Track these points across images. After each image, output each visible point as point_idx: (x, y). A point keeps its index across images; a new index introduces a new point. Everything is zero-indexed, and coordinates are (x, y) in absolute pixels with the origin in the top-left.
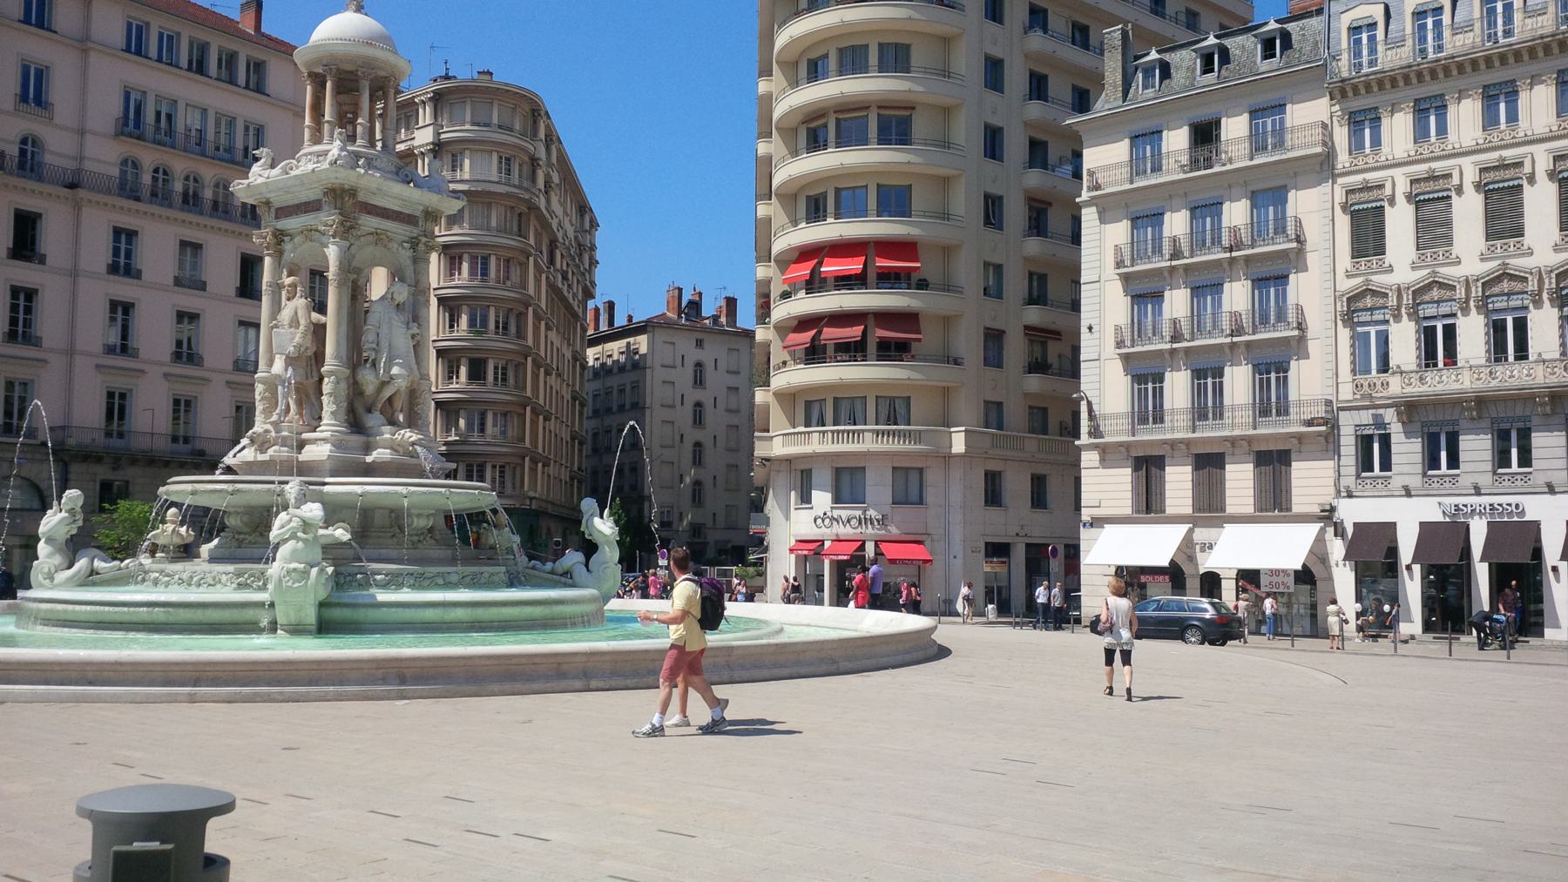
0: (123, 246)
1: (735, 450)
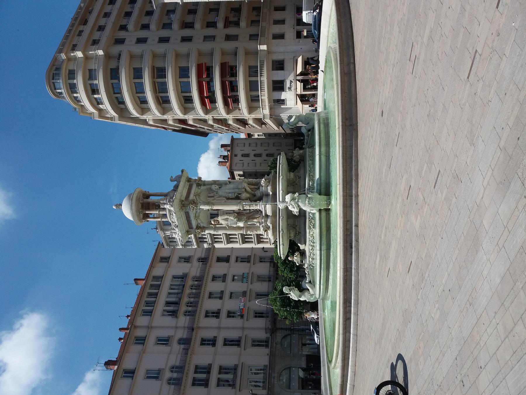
1: (269, 144)
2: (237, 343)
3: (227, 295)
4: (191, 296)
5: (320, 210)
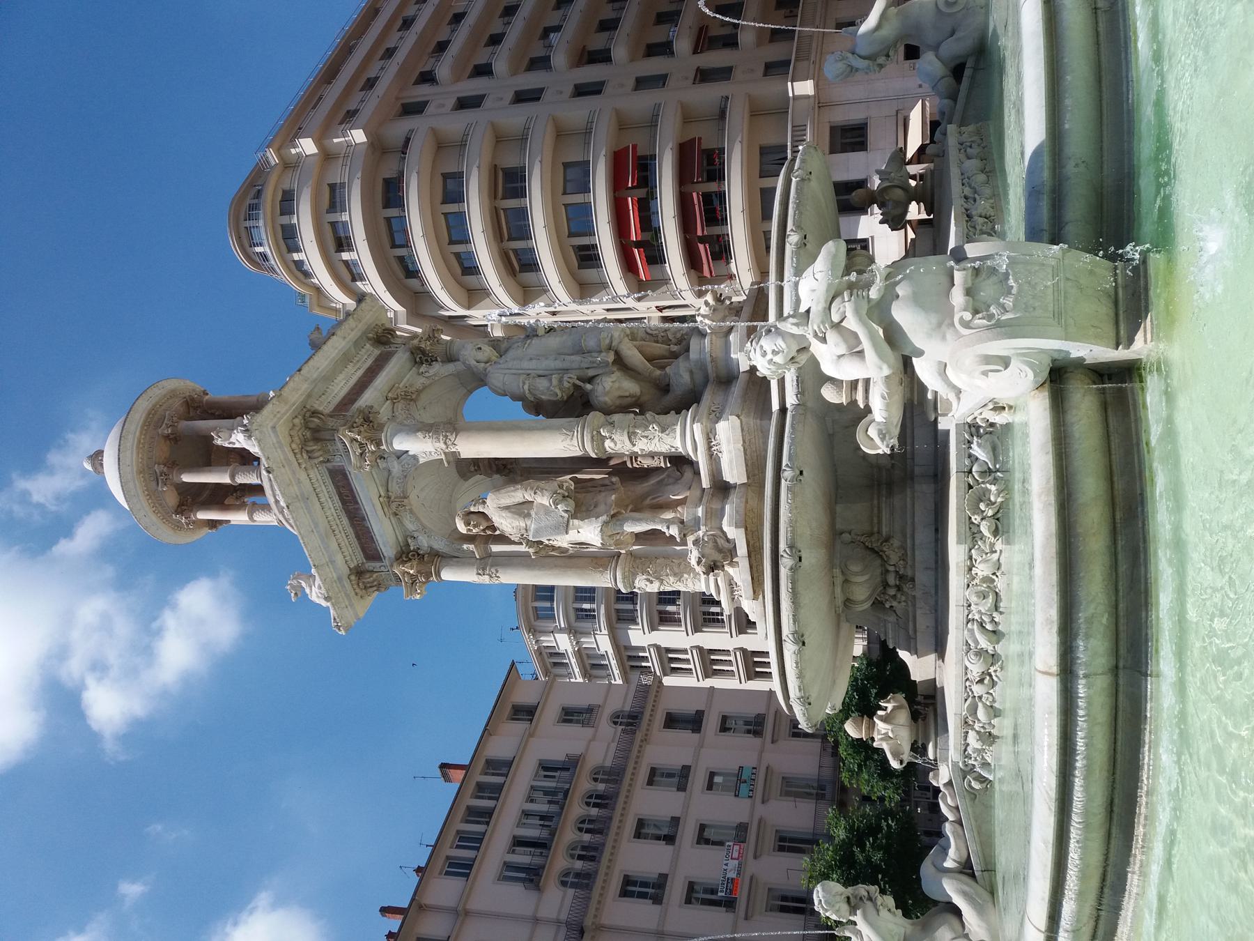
0: (637, 889)
3: (688, 833)
4: (585, 826)
5: (1058, 376)
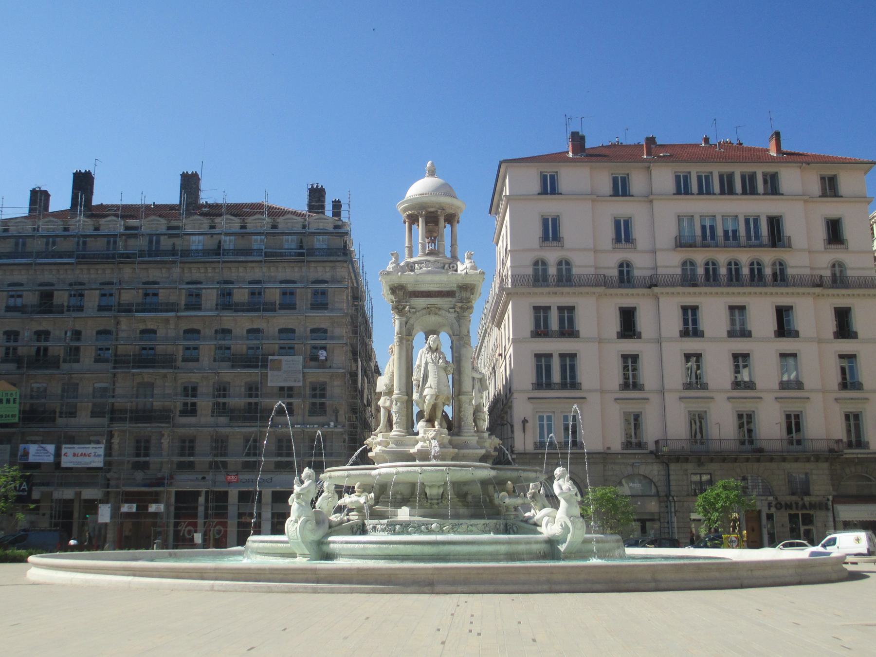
0: (690, 317)
2: (631, 382)
3: (740, 345)
